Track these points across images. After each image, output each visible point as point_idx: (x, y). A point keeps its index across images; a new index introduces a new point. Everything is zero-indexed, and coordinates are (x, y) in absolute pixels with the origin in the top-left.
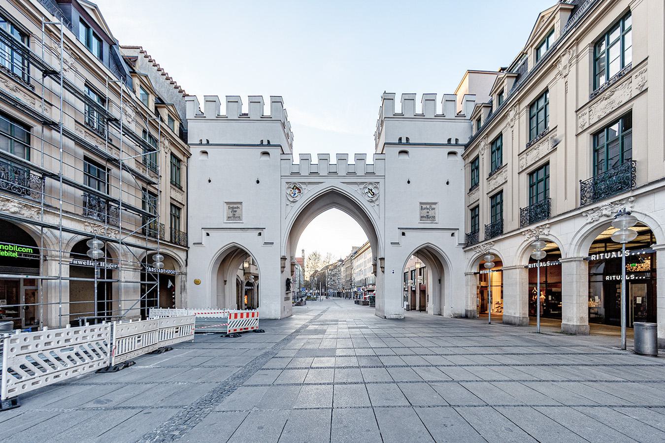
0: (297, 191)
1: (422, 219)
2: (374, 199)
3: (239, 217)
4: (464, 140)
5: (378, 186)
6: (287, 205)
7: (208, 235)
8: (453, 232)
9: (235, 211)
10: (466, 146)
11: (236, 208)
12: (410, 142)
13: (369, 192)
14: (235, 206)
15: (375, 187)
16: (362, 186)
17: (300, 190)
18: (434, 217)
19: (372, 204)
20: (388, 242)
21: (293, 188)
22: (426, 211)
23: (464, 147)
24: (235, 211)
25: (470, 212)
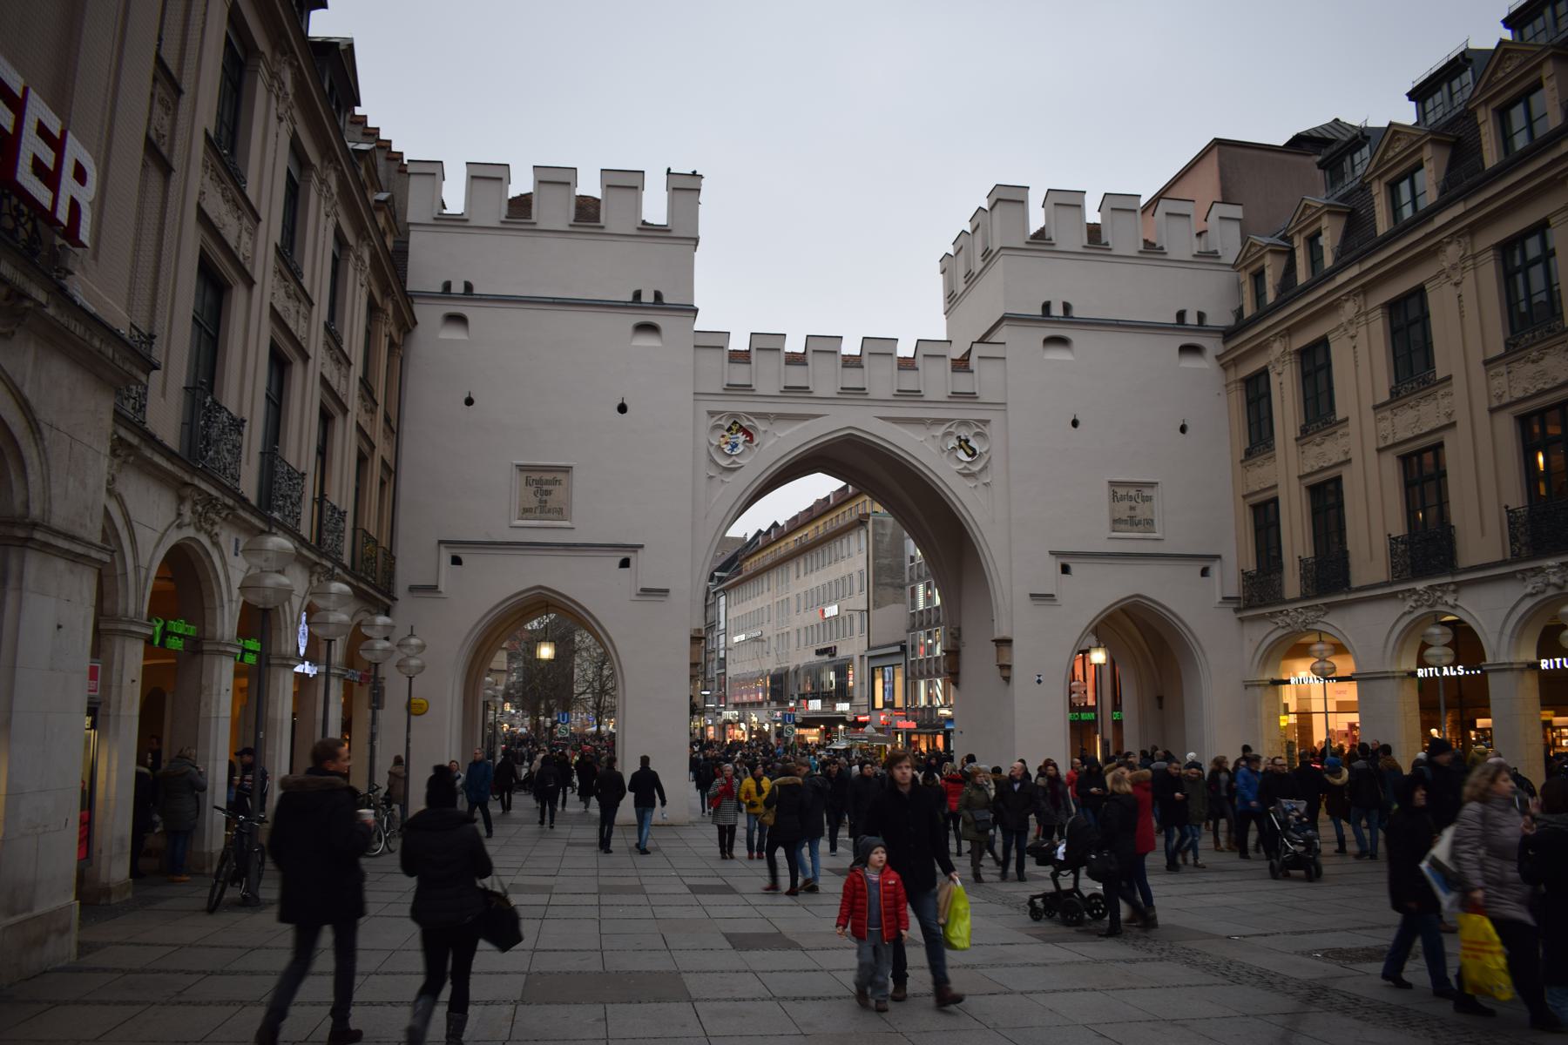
0: (741, 437)
3: (560, 511)
5: (986, 430)
6: (711, 477)
8: (1205, 563)
9: (548, 493)
11: (548, 482)
14: (548, 476)
15: (977, 434)
16: (940, 431)
18: (1150, 522)
21: (729, 429)
22: (1126, 504)
24: (548, 493)
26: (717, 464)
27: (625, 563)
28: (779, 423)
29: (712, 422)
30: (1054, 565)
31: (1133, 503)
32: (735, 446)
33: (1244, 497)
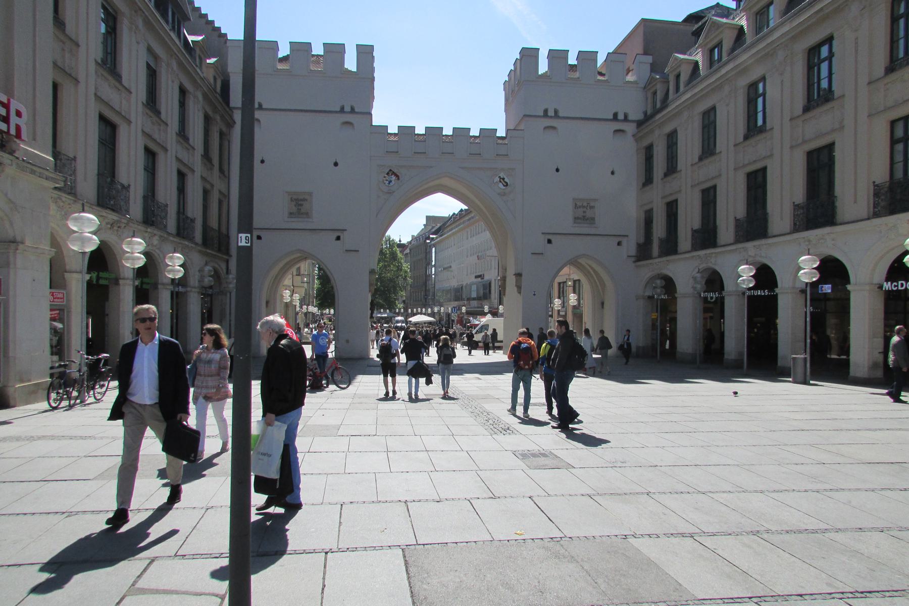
0: (394, 178)
3: (307, 214)
9: (301, 205)
10: (640, 124)
11: (301, 200)
12: (561, 114)
18: (593, 219)
21: (388, 174)
22: (581, 210)
24: (301, 205)
27: (338, 238)
30: (543, 239)
32: (390, 182)
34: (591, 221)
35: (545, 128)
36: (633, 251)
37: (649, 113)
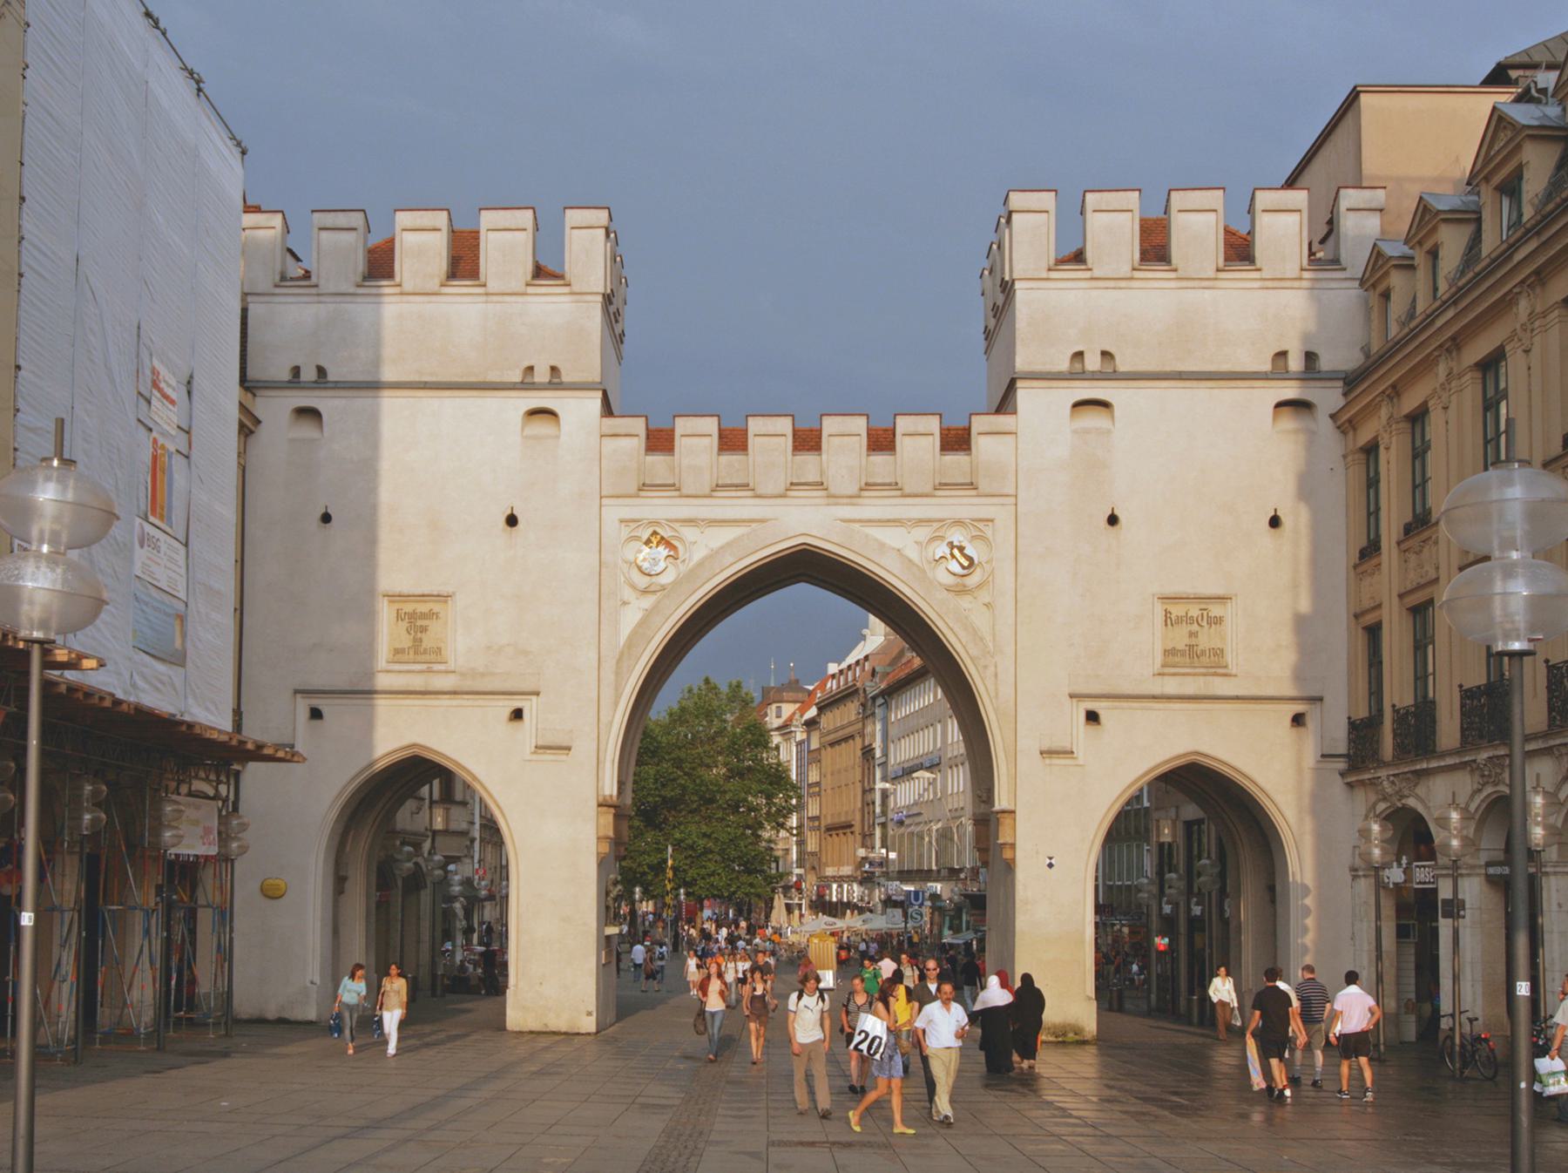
0: (663, 551)
1: (1171, 659)
2: (973, 580)
4: (1341, 356)
5: (989, 534)
6: (625, 603)
7: (316, 714)
10: (1351, 381)
11: (424, 616)
13: (953, 556)
16: (922, 533)
17: (674, 548)
18: (1219, 653)
19: (965, 602)
20: (1029, 744)
21: (648, 542)
22: (1183, 630)
23: (1340, 383)
24: (424, 629)
25: (1361, 640)
26: (633, 587)
28: (710, 531)
29: (625, 532)
31: (1195, 627)
33: (1356, 616)
34: (1215, 663)
35: (1077, 405)
36: (1339, 739)
37: (1375, 348)
